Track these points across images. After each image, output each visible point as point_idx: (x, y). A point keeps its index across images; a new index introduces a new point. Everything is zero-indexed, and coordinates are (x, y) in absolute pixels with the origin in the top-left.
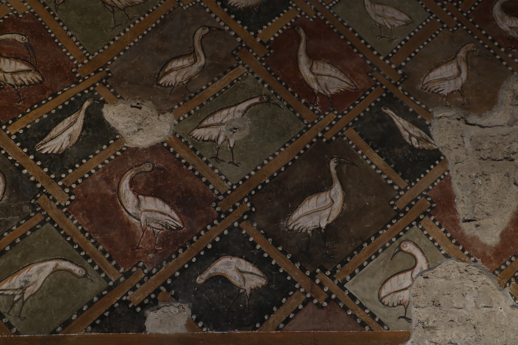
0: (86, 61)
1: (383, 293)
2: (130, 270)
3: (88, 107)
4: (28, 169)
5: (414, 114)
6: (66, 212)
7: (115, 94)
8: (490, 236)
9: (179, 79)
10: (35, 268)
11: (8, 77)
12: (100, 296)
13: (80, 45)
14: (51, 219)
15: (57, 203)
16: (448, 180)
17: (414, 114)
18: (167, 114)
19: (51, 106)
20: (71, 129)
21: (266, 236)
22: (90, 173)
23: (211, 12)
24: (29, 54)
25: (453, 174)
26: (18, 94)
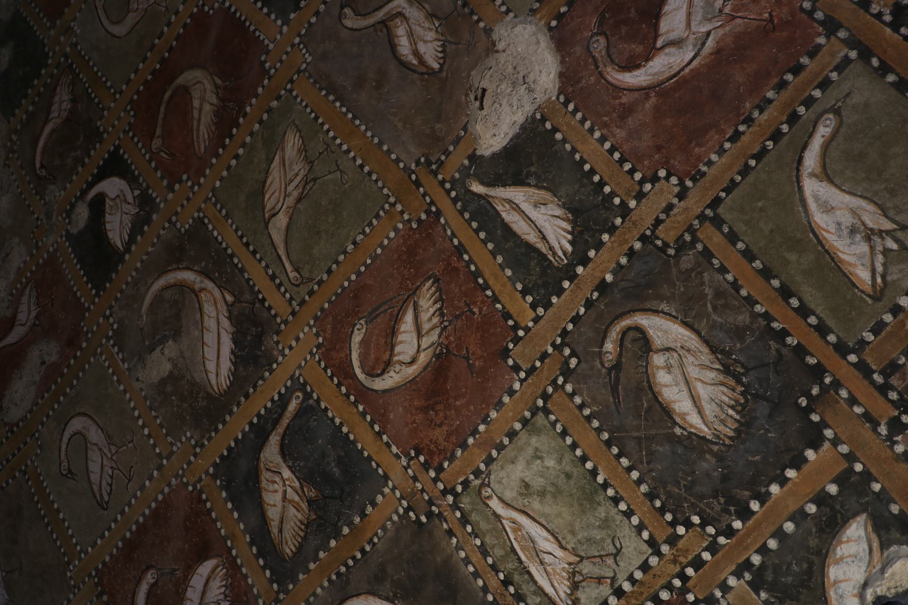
0: (399, 207)
2: (822, 23)
3: (483, 183)
4: (604, 272)
6: (694, 179)
7: (457, 141)
9: (431, 35)
10: (820, 218)
11: (426, 342)
12: (885, 69)
13: (370, 224)
14: (708, 206)
15: (675, 201)
18: (495, 37)
20: (525, 207)
22: (611, 151)
23: (317, 13)
24: (386, 311)
26: (457, 317)
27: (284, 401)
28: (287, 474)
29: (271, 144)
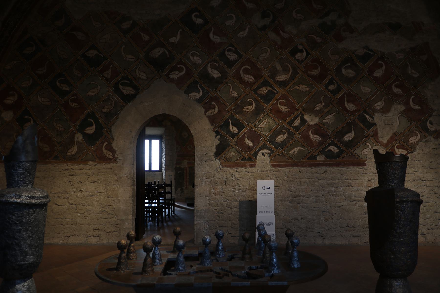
8: (385, 141)
16: (377, 129)
19: (293, 116)
25: (378, 128)
27: (275, 90)
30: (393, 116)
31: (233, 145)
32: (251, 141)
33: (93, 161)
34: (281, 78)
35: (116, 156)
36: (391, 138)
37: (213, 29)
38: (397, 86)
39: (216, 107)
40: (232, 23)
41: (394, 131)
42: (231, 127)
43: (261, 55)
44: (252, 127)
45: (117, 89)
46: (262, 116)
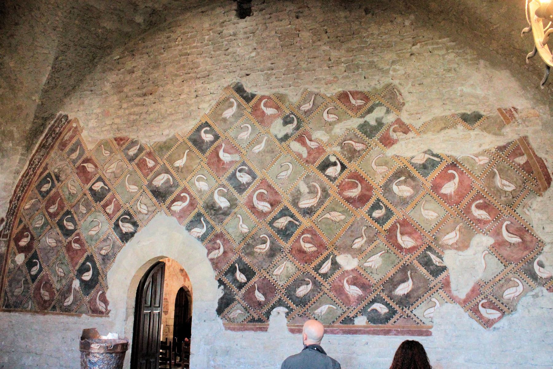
1: (425, 314)
5: (438, 253)
8: (462, 295)
10: (323, 307)
12: (342, 315)
16: (448, 276)
17: (438, 253)
19: (321, 258)
21: (388, 297)
27: (297, 220)
28: (286, 223)
29: (343, 212)
30: (474, 254)
31: (240, 299)
32: (263, 294)
33: (86, 314)
34: (306, 203)
35: (109, 308)
36: (473, 291)
37: (223, 145)
38: (478, 207)
39: (222, 246)
40: (246, 136)
41: (478, 278)
42: (238, 273)
43: (281, 174)
44: (265, 274)
45: (117, 226)
46: (278, 258)
